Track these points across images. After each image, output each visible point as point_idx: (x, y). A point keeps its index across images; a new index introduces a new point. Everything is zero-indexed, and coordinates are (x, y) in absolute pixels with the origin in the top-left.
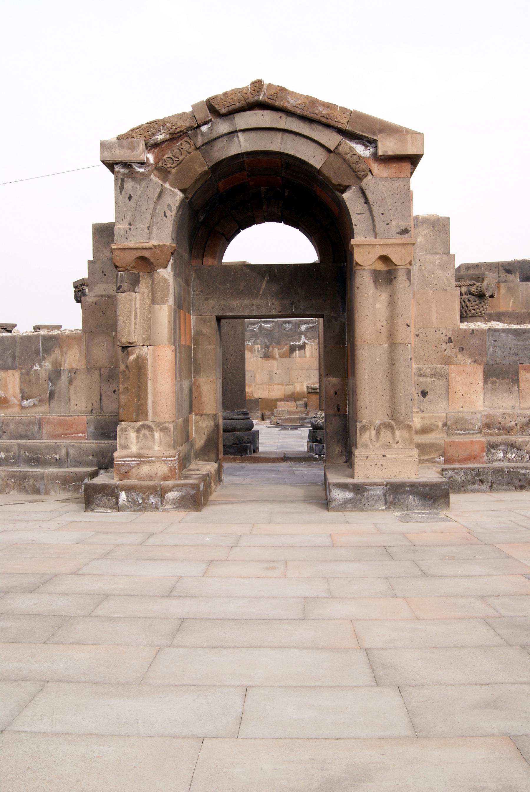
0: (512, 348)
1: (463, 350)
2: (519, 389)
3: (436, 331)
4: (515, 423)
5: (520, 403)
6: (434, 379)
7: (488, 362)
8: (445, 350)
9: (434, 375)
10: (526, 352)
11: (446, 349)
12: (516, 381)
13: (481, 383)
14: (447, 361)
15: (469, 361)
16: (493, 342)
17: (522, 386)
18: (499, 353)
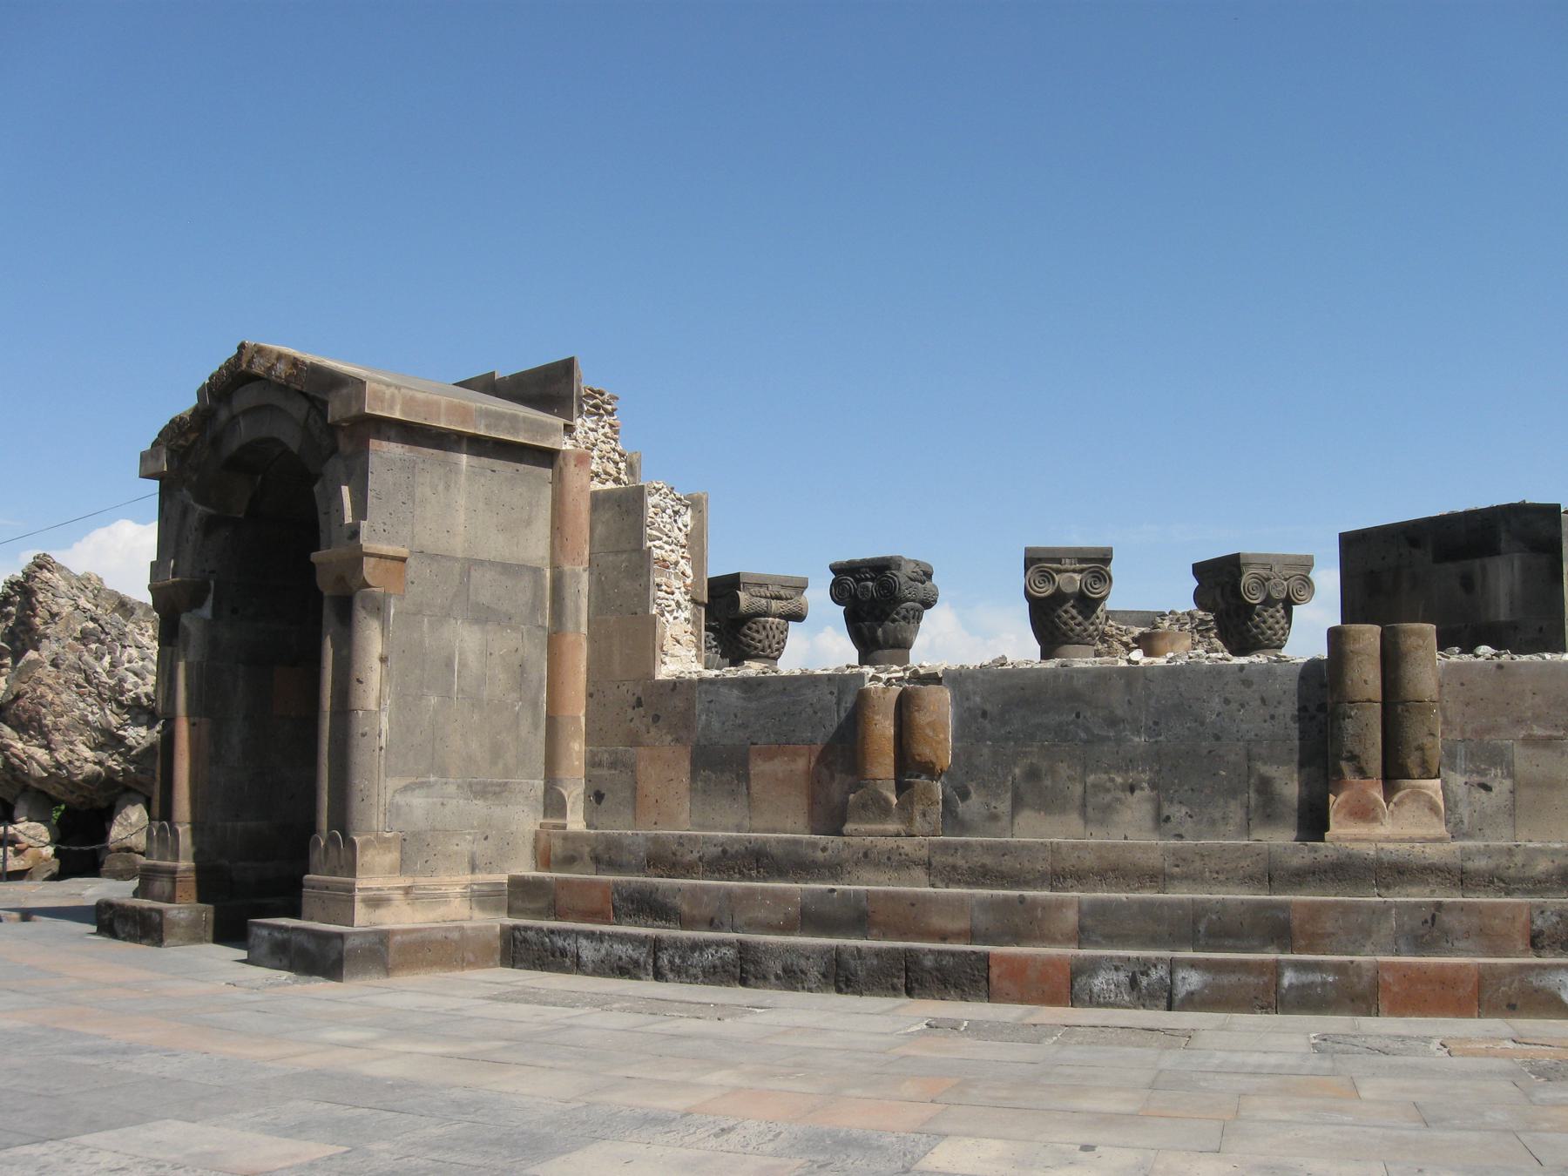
0: (739, 715)
1: (659, 719)
2: (749, 793)
3: (618, 687)
4: (698, 855)
5: (750, 818)
6: (613, 772)
7: (698, 741)
8: (631, 720)
9: (613, 765)
10: (762, 722)
11: (633, 718)
12: (744, 777)
13: (685, 779)
14: (634, 741)
15: (669, 738)
16: (707, 705)
18: (716, 725)
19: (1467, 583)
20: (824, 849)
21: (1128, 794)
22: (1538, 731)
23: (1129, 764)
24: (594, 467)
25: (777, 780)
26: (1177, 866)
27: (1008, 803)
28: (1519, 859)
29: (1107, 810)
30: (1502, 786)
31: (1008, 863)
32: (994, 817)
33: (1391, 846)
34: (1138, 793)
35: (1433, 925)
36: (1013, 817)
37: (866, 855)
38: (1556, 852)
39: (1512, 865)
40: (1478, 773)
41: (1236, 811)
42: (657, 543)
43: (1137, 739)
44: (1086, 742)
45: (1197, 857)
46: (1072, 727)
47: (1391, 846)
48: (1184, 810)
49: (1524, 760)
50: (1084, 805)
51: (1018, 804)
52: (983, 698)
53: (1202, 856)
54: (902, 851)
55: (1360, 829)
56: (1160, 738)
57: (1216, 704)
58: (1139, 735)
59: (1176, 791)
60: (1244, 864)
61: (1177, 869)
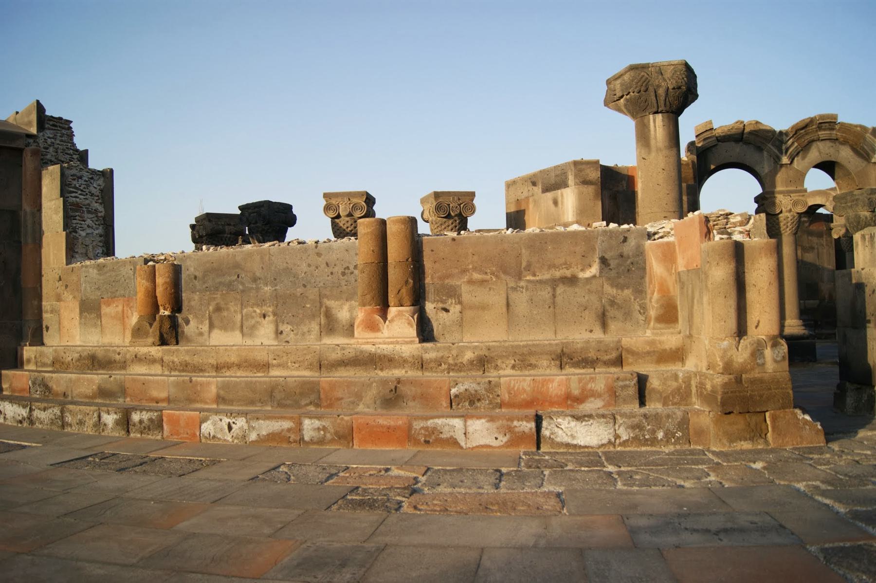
6: (52, 315)
12: (99, 316)
17: (104, 320)
19: (555, 203)
20: (119, 354)
21: (263, 319)
22: (476, 276)
23: (262, 302)
24: (49, 157)
25: (112, 317)
26: (275, 359)
27: (207, 326)
28: (454, 352)
29: (253, 327)
30: (455, 309)
31: (197, 360)
32: (201, 334)
33: (384, 346)
34: (267, 318)
35: (396, 392)
36: (210, 332)
37: (136, 356)
38: (476, 347)
39: (451, 356)
40: (441, 302)
41: (315, 327)
42: (73, 195)
43: (266, 288)
44: (243, 291)
45: (285, 354)
46: (236, 282)
47: (384, 346)
48: (289, 327)
49: (466, 294)
50: (242, 326)
51: (212, 326)
52: (195, 268)
53: (287, 353)
54: (151, 354)
55: (370, 335)
56: (277, 288)
57: (304, 267)
58: (267, 286)
59: (285, 317)
60: (308, 357)
61: (275, 361)
